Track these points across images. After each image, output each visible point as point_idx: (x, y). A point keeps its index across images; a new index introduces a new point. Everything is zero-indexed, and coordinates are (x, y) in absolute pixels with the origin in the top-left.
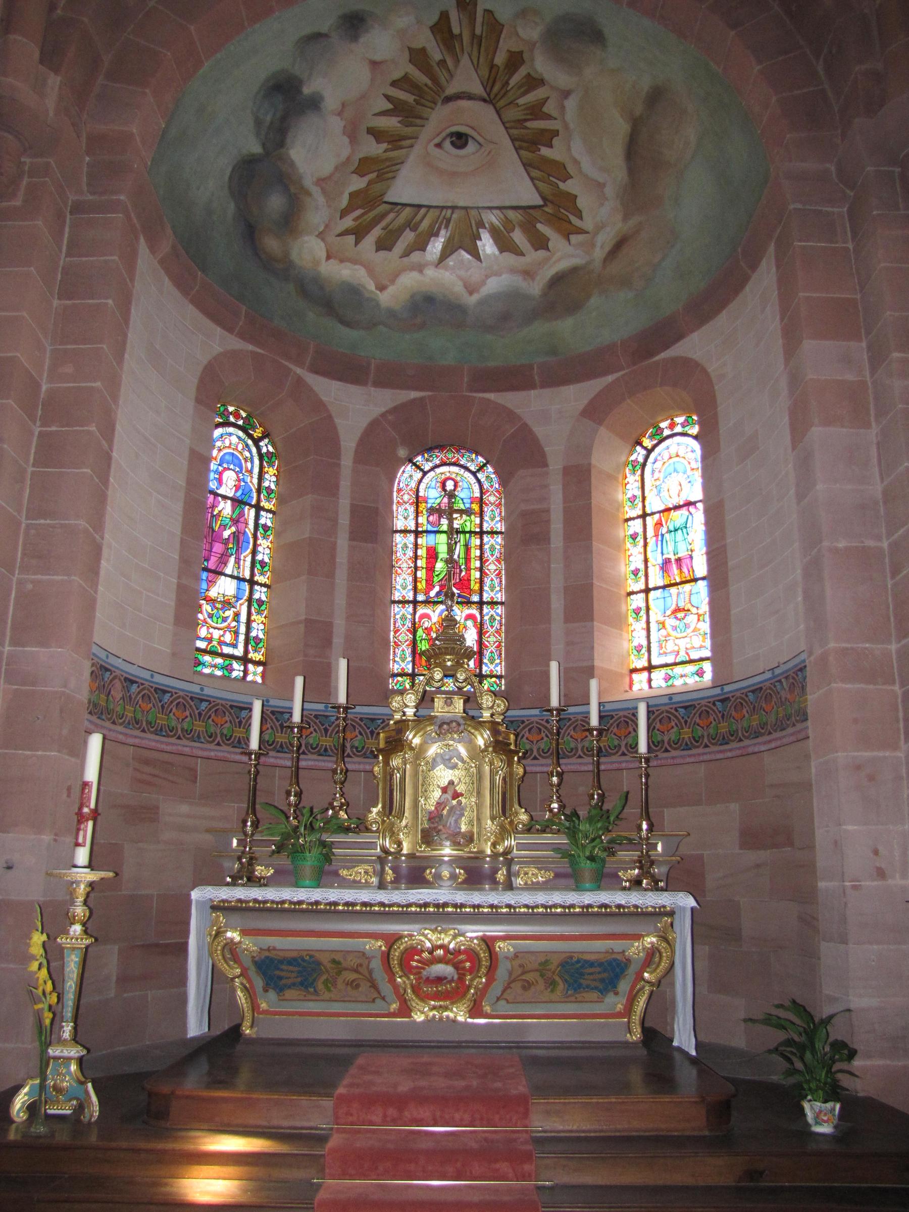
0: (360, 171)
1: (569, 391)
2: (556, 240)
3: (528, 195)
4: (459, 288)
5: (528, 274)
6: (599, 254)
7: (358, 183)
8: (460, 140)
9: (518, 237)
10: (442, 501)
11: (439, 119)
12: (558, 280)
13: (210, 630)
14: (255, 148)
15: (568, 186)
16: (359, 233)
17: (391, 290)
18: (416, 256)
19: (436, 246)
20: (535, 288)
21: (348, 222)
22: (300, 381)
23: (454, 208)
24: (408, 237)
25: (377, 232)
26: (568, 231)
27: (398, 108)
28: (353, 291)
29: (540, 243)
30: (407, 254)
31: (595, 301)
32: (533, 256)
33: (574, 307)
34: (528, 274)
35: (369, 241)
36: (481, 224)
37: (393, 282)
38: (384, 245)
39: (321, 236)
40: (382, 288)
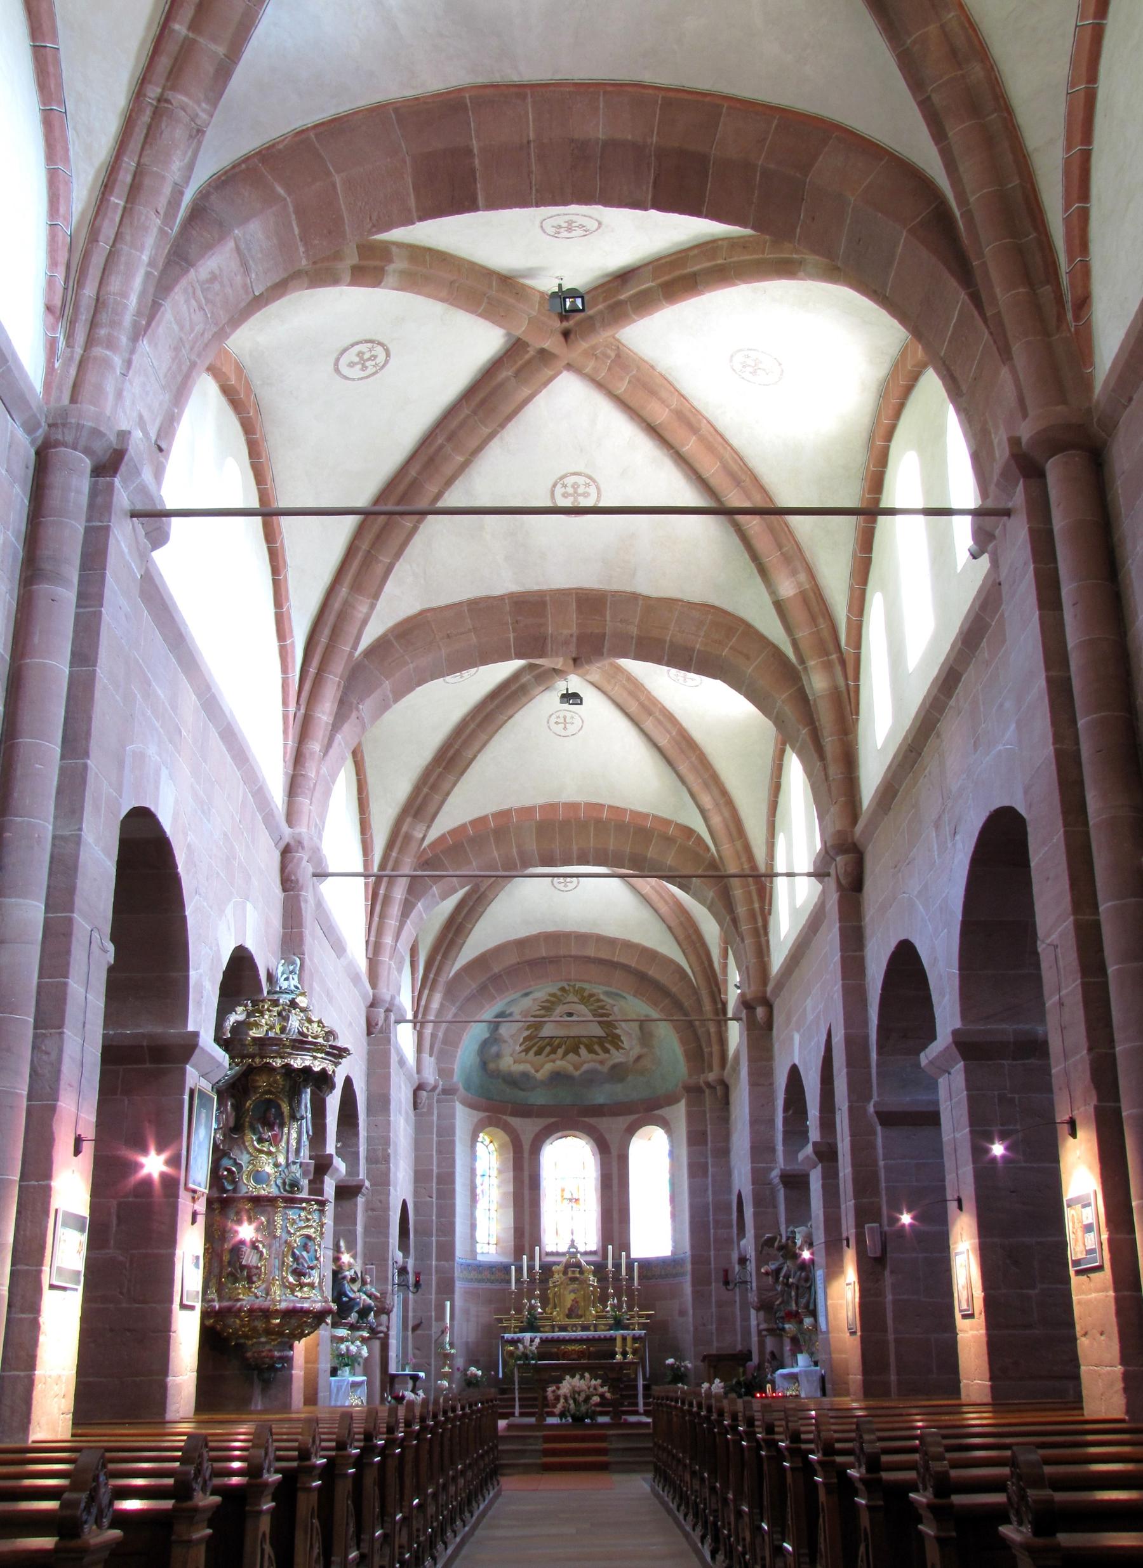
0: (528, 1029)
1: (621, 1119)
2: (613, 1050)
3: (599, 1032)
4: (570, 1068)
5: (602, 1063)
6: (632, 1059)
7: (527, 1033)
8: (570, 1015)
9: (597, 1048)
10: (568, 1162)
11: (560, 1009)
12: (614, 1067)
13: (481, 1235)
14: (487, 1035)
15: (618, 1031)
16: (527, 1051)
17: (541, 1072)
18: (553, 1056)
19: (560, 1051)
20: (605, 1069)
21: (523, 1047)
22: (506, 1121)
23: (568, 1037)
24: (548, 1049)
25: (535, 1049)
26: (618, 1048)
27: (543, 1008)
28: (525, 1075)
29: (607, 1051)
30: (548, 1055)
31: (630, 1078)
32: (603, 1056)
33: (621, 1080)
34: (602, 1063)
35: (532, 1053)
36: (580, 1043)
37: (542, 1067)
38: (538, 1053)
39: (511, 1055)
40: (537, 1071)
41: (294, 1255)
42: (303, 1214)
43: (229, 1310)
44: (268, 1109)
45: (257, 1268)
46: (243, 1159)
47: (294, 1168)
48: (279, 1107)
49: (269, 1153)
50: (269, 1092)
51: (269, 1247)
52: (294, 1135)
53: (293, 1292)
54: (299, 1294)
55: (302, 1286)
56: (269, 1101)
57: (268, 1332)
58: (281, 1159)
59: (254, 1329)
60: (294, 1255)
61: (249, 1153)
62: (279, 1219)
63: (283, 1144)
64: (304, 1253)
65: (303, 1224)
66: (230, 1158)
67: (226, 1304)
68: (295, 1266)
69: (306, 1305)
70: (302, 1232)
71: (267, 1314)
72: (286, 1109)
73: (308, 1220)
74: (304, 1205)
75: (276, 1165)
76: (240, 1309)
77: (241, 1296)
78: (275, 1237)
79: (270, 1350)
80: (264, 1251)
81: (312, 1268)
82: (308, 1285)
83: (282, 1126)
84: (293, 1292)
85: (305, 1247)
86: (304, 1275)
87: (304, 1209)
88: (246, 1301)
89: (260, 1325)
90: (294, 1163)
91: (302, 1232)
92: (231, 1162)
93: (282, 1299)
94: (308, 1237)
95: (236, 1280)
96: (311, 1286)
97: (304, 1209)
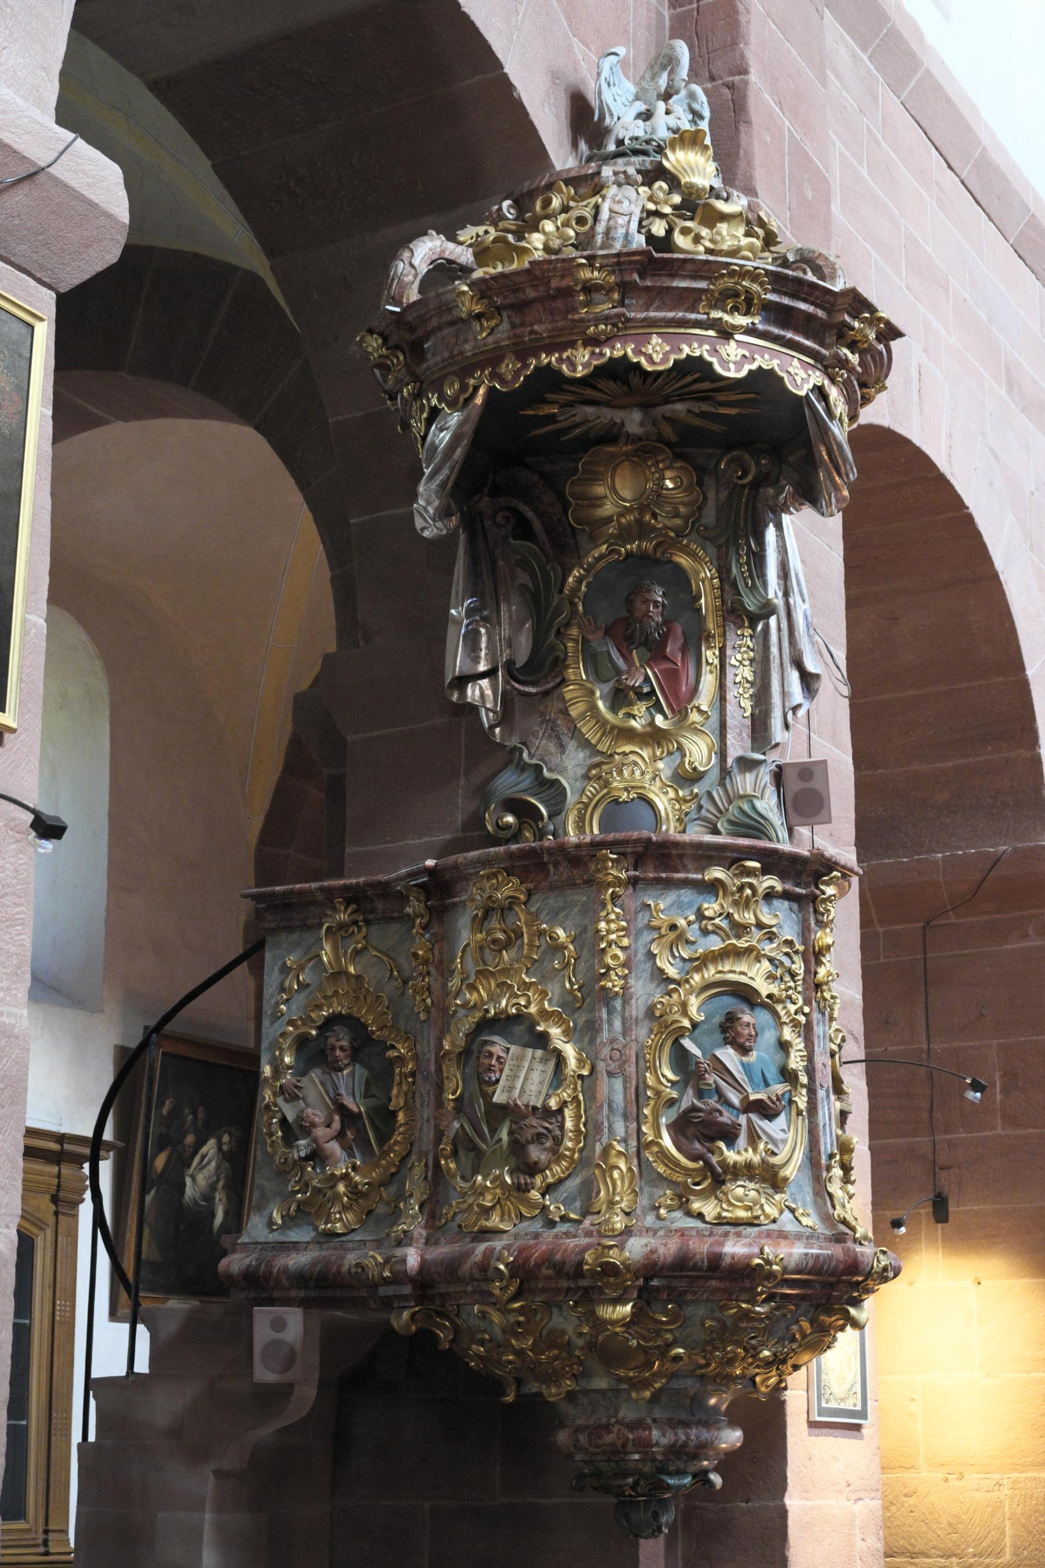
41: (681, 1059)
42: (712, 907)
43: (451, 1269)
44: (637, 591)
45: (547, 1113)
46: (569, 767)
47: (745, 782)
48: (680, 584)
49: (654, 737)
50: (642, 531)
51: (586, 1034)
52: (742, 672)
53: (682, 1203)
54: (709, 1209)
55: (718, 1178)
56: (643, 558)
57: (606, 1350)
58: (699, 750)
59: (554, 1340)
60: (681, 1059)
61: (585, 744)
62: (610, 924)
63: (705, 698)
64: (728, 1056)
65: (715, 943)
66: (523, 767)
67: (443, 1250)
68: (689, 1099)
69: (735, 1248)
70: (710, 973)
71: (583, 1282)
72: (705, 576)
73: (740, 929)
74: (717, 873)
75: (687, 778)
76: (485, 1270)
77: (495, 1221)
78: (606, 997)
79: (638, 1424)
80: (570, 1051)
81: (766, 1110)
82: (748, 1171)
83: (693, 644)
84: (682, 1203)
85: (729, 1031)
86: (730, 1136)
87: (714, 888)
88: (509, 1236)
89: (566, 1322)
90: (747, 764)
91: (710, 973)
92: (527, 780)
93: (642, 1232)
94: (746, 995)
95: (479, 1163)
96: (771, 1178)
97: (714, 888)
